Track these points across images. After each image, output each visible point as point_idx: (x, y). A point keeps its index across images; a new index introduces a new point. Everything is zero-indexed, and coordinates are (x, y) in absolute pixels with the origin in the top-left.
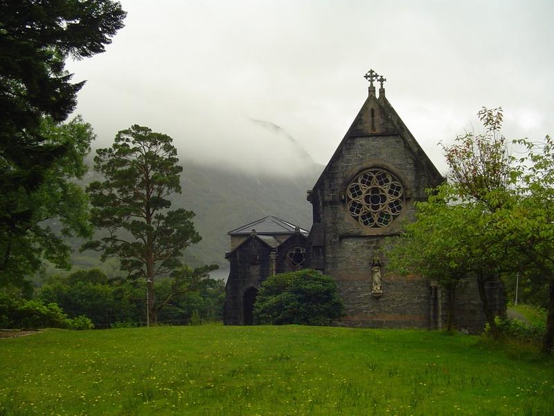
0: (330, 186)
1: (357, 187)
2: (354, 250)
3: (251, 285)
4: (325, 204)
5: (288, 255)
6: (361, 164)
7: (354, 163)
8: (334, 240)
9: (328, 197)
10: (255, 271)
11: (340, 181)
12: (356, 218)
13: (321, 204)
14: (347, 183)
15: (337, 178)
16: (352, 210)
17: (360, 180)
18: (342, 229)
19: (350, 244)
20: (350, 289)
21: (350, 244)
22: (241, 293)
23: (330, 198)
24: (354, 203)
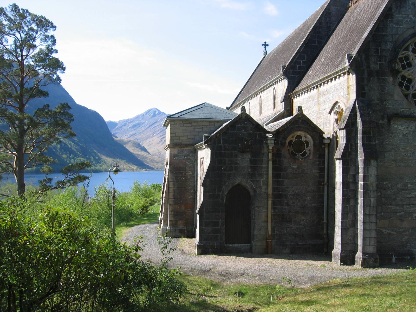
0: (377, 51)
1: (407, 58)
2: (404, 135)
3: (238, 180)
4: (370, 74)
5: (287, 142)
6: (413, 28)
7: (405, 26)
8: (381, 122)
9: (374, 66)
10: (244, 161)
11: (389, 46)
12: (406, 96)
13: (366, 74)
14: (395, 51)
15: (386, 42)
16: (401, 85)
17: (411, 49)
18: (391, 107)
19: (400, 127)
20: (399, 186)
21: (400, 127)
22: (226, 190)
23: (377, 67)
24: (404, 78)
